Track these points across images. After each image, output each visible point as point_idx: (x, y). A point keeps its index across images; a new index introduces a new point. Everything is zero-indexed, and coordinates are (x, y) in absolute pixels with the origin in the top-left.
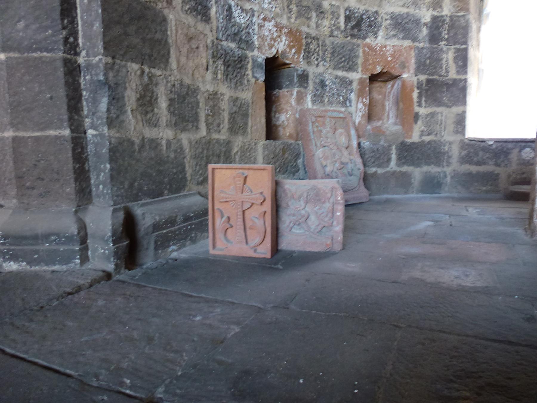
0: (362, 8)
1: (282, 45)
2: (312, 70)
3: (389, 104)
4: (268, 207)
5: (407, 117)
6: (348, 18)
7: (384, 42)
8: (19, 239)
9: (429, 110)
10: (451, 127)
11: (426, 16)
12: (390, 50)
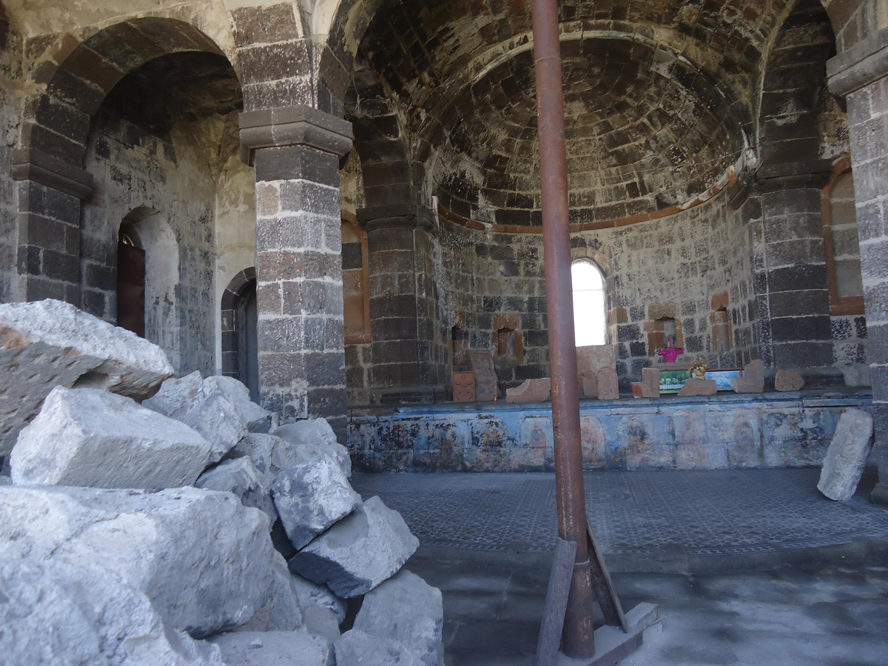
0: (492, 296)
1: (457, 321)
2: (470, 330)
3: (509, 345)
4: (473, 385)
5: (519, 352)
6: (485, 302)
7: (505, 312)
8: (406, 394)
9: (531, 348)
10: (545, 357)
11: (526, 298)
12: (508, 316)
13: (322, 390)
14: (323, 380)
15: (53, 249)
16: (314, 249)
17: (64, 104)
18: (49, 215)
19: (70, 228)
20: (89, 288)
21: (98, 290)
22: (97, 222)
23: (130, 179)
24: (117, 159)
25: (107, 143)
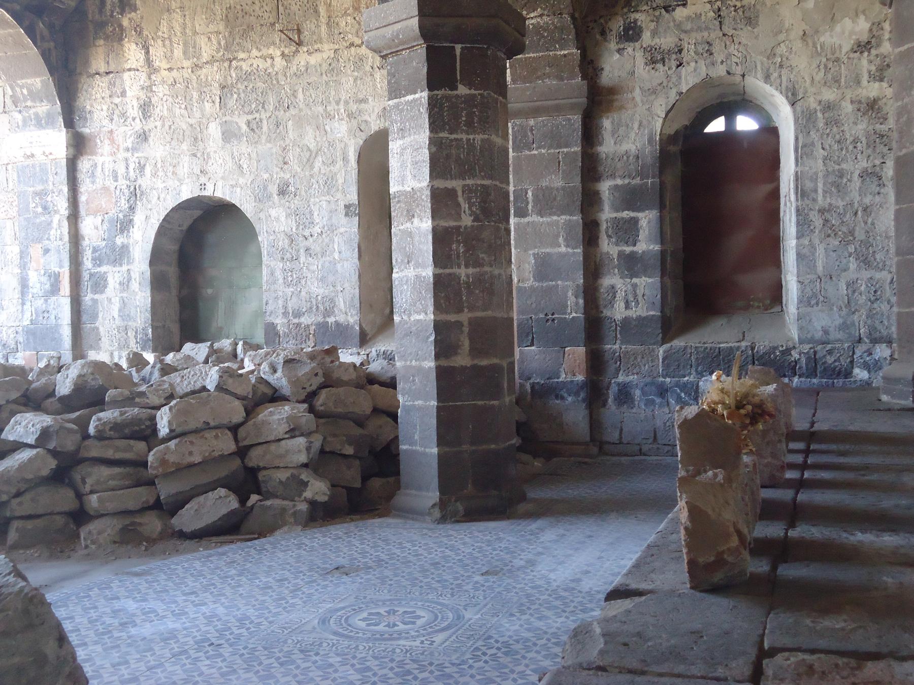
13: (411, 367)
14: (411, 354)
15: (544, 183)
16: (401, 188)
17: (533, 21)
18: (537, 149)
19: (567, 154)
20: (614, 215)
21: (626, 214)
22: (622, 131)
23: (680, 51)
24: (654, 33)
25: (636, 21)
